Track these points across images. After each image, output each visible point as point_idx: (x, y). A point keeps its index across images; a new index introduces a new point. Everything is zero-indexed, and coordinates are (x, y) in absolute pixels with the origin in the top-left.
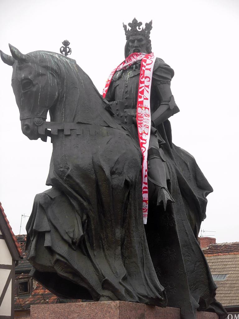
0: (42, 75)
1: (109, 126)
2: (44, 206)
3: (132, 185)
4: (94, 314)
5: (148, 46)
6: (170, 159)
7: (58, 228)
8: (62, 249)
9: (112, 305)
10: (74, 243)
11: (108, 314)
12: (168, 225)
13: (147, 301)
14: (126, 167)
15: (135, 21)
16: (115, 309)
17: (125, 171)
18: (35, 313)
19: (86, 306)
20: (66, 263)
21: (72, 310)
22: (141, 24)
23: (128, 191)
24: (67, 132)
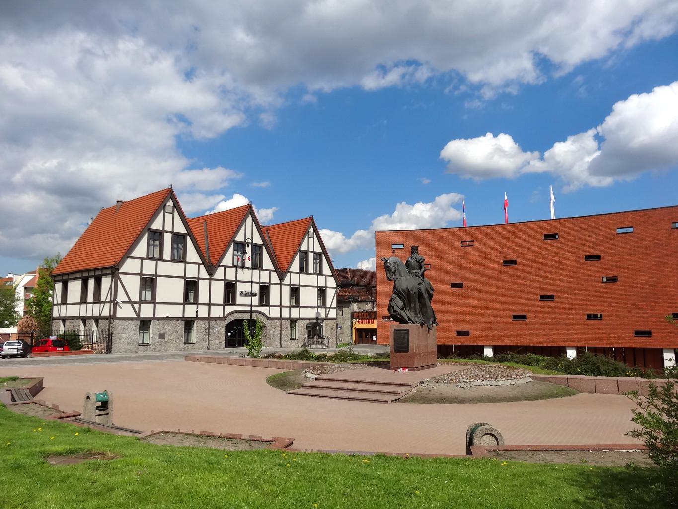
8: (398, 310)
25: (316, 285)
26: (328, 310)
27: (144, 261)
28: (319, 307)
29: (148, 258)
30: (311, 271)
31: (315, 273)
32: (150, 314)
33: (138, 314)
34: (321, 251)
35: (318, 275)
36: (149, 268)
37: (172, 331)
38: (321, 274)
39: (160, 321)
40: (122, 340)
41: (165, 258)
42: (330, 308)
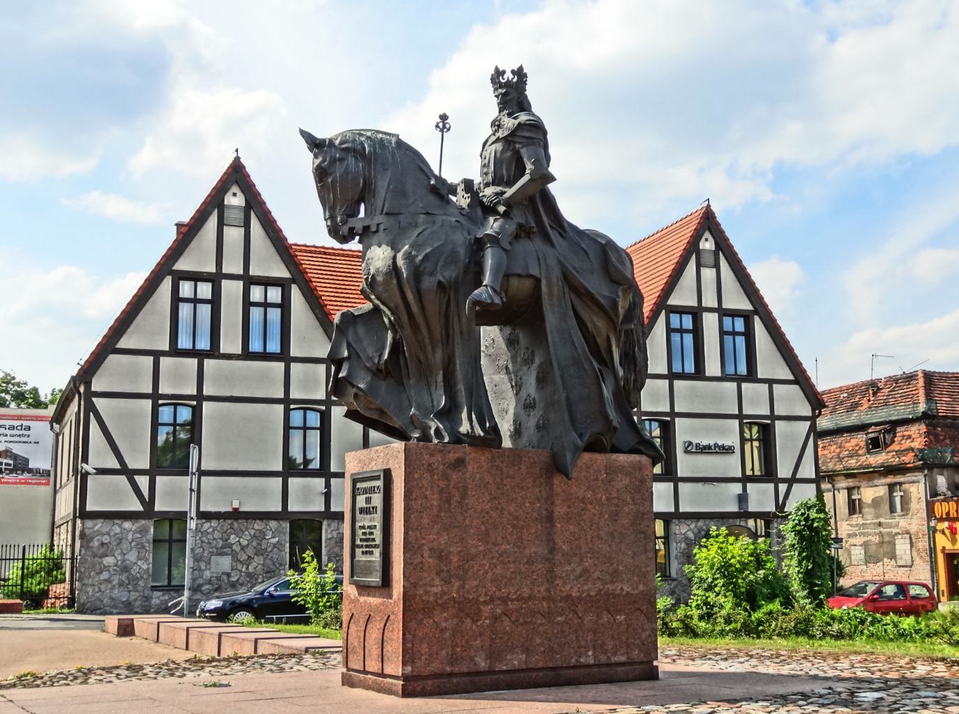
0: (341, 160)
1: (427, 214)
3: (450, 287)
5: (522, 98)
6: (551, 248)
7: (360, 354)
10: (379, 370)
14: (440, 264)
15: (497, 69)
17: (439, 269)
22: (504, 72)
24: (374, 229)
26: (783, 488)
27: (163, 360)
28: (745, 480)
29: (175, 352)
30: (713, 367)
31: (724, 378)
32: (184, 504)
33: (149, 504)
34: (746, 305)
35: (739, 379)
36: (178, 377)
37: (250, 551)
38: (751, 376)
39: (214, 523)
40: (105, 576)
41: (224, 349)
42: (792, 481)
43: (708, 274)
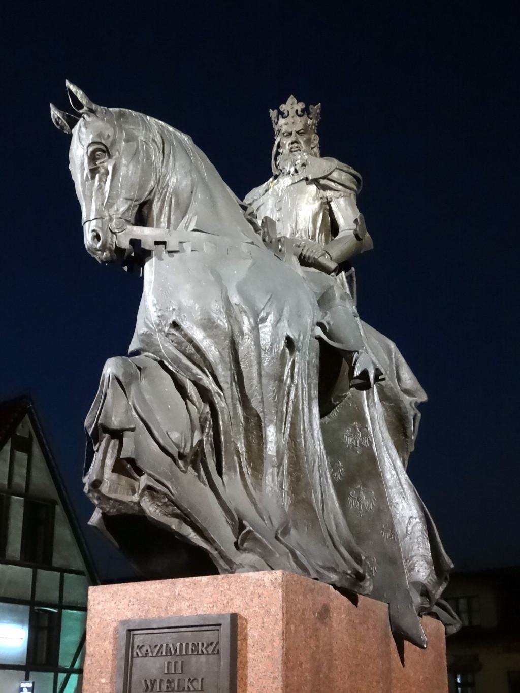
1: (252, 243)
2: (121, 378)
4: (225, 602)
9: (265, 579)
10: (182, 456)
11: (256, 599)
12: (358, 445)
13: (334, 577)
16: (272, 589)
18: (98, 604)
19: (207, 585)
20: (166, 495)
21: (177, 594)
23: (292, 360)
24: (172, 245)
25: (29, 597)
43: (21, 456)
